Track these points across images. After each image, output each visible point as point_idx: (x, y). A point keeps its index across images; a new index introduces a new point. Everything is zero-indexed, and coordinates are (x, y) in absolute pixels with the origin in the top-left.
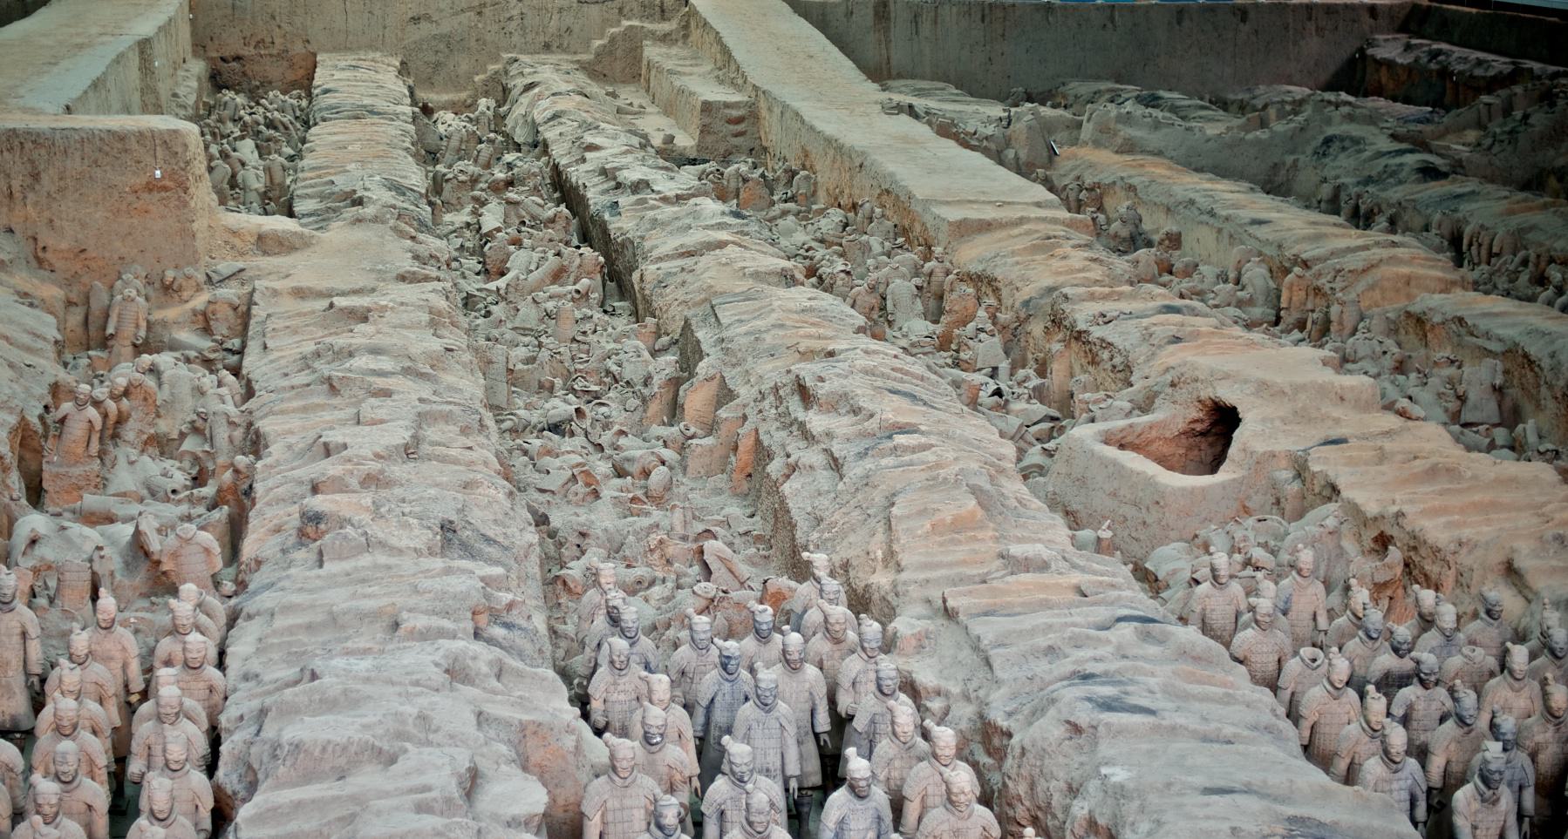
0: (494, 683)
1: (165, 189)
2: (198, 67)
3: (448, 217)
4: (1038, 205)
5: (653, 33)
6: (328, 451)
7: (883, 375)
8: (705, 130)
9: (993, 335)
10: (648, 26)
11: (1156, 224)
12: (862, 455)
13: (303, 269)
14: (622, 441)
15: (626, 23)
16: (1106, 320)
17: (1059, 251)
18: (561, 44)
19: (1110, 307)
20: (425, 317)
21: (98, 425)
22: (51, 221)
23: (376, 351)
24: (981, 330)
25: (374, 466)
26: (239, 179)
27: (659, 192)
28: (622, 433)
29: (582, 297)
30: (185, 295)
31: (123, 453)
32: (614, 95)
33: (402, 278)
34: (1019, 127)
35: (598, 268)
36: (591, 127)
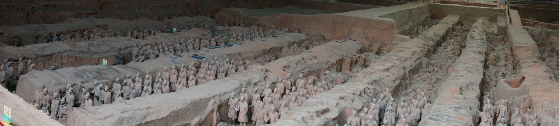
0: (350, 101)
1: (387, 29)
2: (428, 14)
3: (449, 40)
6: (372, 68)
13: (406, 44)
14: (438, 75)
20: (412, 52)
21: (350, 61)
22: (370, 33)
23: (395, 56)
25: (374, 71)
26: (418, 31)
28: (438, 74)
29: (454, 53)
30: (388, 46)
31: (357, 66)
33: (418, 47)
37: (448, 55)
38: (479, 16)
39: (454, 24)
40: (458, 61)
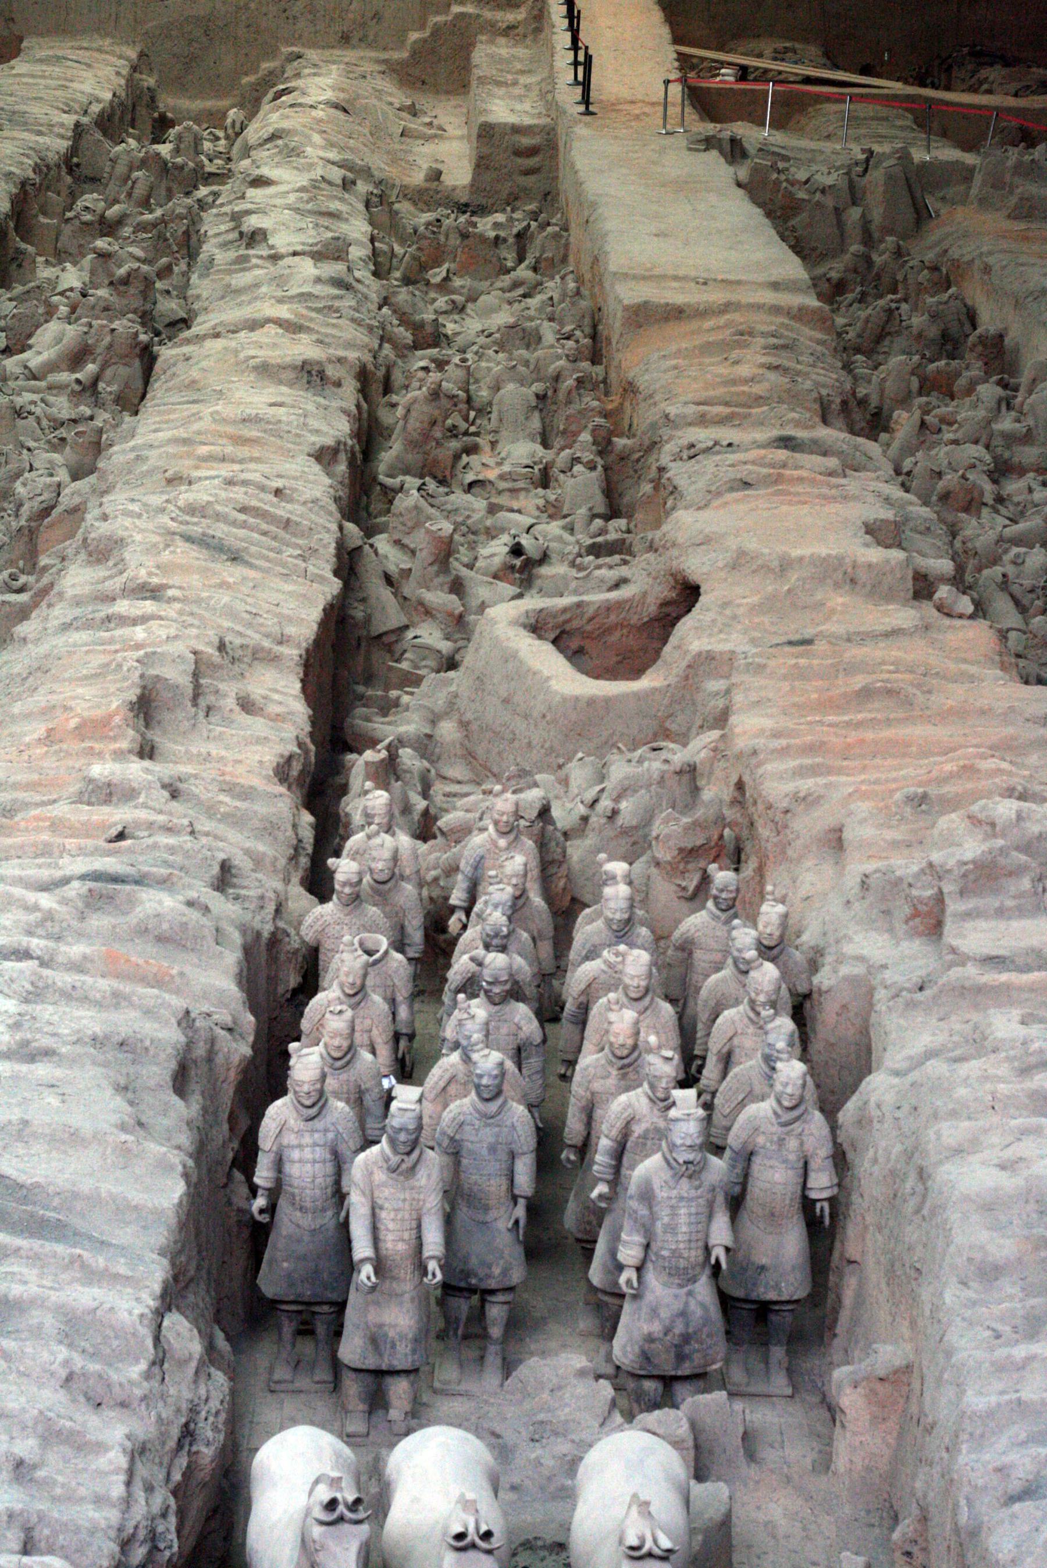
3: (45, 273)
4: (775, 286)
5: (492, 24)
7: (218, 517)
8: (482, 164)
9: (593, 468)
10: (488, 14)
11: (989, 321)
12: (66, 627)
15: (456, 9)
16: (693, 451)
17: (734, 355)
18: (366, 36)
19: (702, 436)
24: (576, 460)
27: (272, 247)
29: (90, 389)
32: (413, 111)
34: (877, 175)
35: (137, 351)
36: (292, 153)
37: (38, 410)
38: (314, 45)
39: (85, 120)
40: (118, 455)
